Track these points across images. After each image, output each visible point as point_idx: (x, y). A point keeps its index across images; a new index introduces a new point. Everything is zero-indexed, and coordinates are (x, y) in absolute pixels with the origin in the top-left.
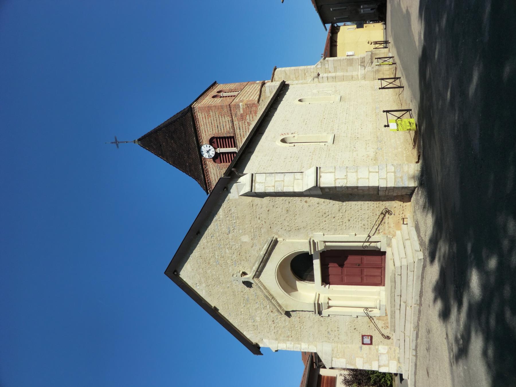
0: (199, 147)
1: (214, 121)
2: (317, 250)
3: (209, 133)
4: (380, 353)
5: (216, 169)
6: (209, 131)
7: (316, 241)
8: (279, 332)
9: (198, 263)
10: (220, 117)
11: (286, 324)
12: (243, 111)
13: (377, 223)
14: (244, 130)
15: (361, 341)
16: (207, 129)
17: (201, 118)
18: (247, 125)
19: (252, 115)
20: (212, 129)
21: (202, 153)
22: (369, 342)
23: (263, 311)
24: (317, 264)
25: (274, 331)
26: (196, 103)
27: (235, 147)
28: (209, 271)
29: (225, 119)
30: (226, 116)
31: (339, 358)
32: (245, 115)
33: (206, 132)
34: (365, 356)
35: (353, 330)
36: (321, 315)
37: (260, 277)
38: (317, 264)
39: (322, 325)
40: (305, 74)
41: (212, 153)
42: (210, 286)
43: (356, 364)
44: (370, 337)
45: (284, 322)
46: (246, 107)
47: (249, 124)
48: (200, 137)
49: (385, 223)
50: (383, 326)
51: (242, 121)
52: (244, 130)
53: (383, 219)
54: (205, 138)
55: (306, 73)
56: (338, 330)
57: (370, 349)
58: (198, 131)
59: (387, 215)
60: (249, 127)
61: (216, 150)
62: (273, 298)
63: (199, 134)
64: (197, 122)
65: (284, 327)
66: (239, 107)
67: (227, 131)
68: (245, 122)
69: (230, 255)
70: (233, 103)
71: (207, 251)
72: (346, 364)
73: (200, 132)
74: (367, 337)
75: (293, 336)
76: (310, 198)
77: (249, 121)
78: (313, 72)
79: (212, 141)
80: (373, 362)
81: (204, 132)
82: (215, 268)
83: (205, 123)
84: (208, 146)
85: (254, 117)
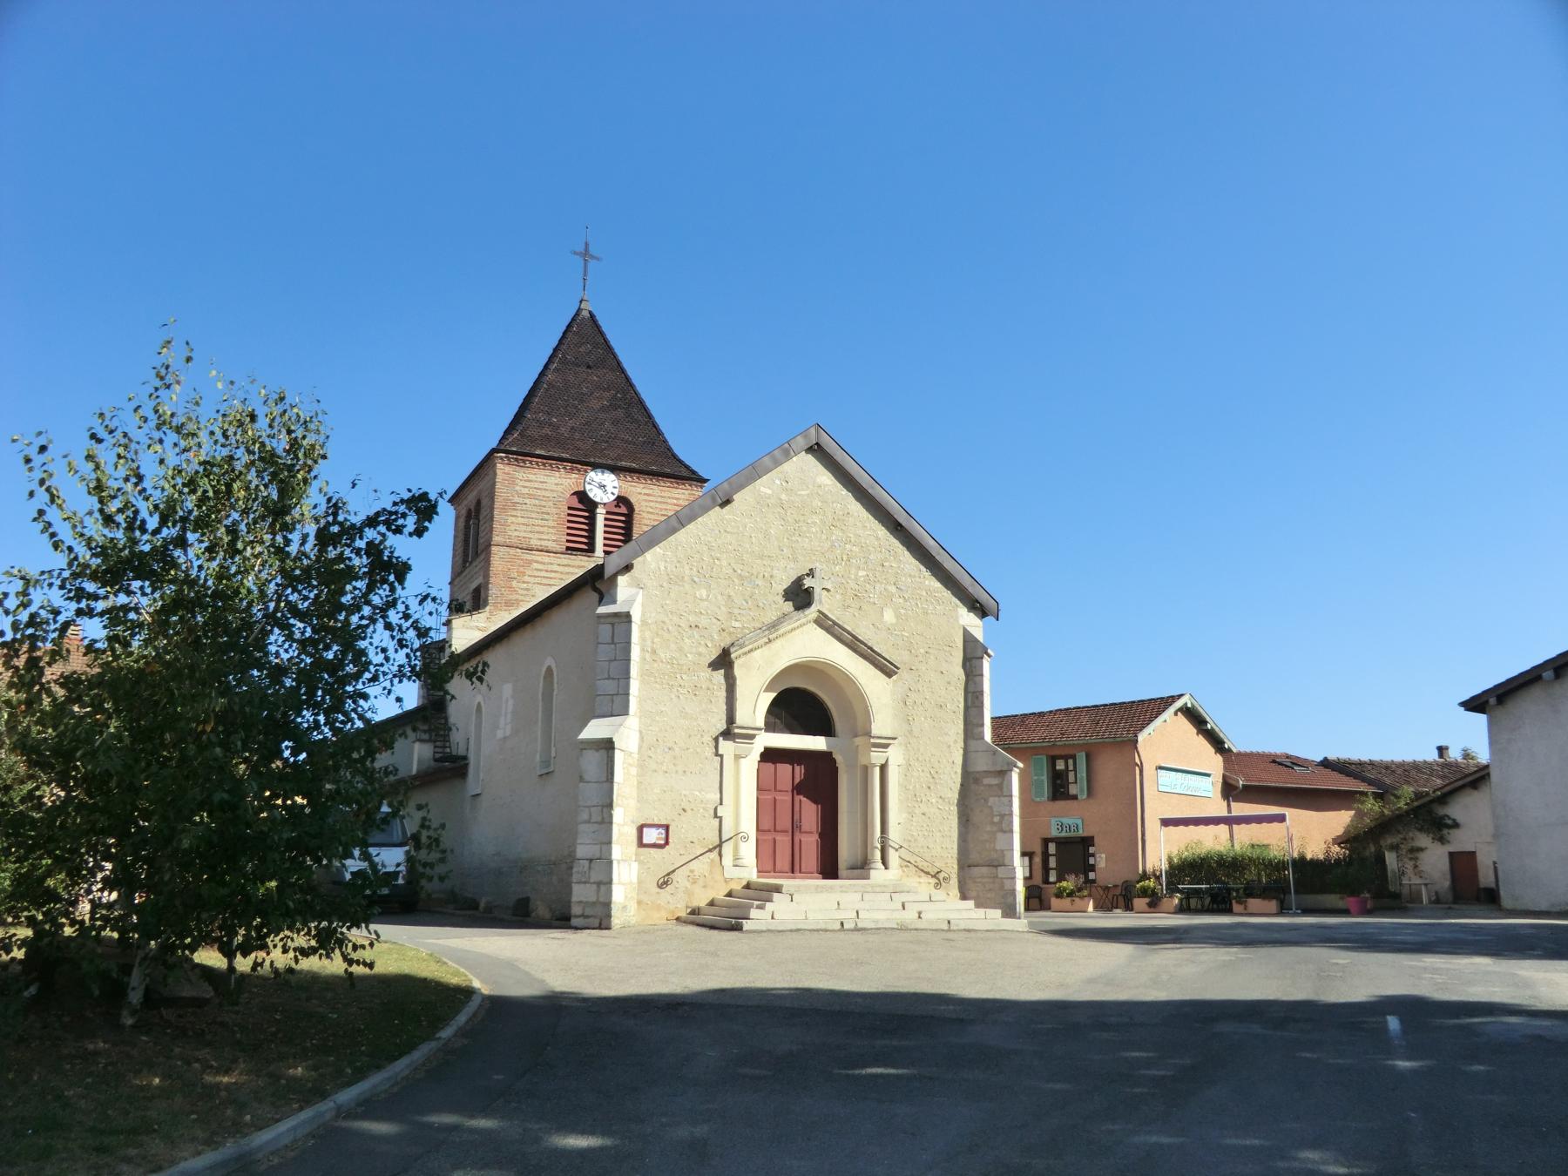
0: (614, 469)
2: (873, 749)
5: (558, 491)
6: (647, 504)
7: (889, 749)
8: (666, 635)
9: (835, 505)
11: (688, 655)
13: (922, 864)
15: (649, 822)
16: (652, 501)
17: (677, 496)
20: (651, 513)
21: (600, 470)
22: (645, 841)
23: (723, 608)
24: (817, 743)
25: (666, 620)
28: (816, 519)
33: (646, 497)
35: (680, 805)
36: (721, 739)
37: (815, 626)
38: (817, 743)
39: (690, 736)
41: (595, 494)
42: (782, 511)
44: (662, 842)
45: (694, 650)
48: (638, 478)
49: (920, 877)
50: (696, 873)
53: (928, 873)
54: (633, 489)
56: (677, 772)
58: (651, 480)
59: (933, 881)
62: (770, 641)
63: (645, 479)
64: (671, 483)
65: (681, 649)
69: (853, 577)
71: (860, 532)
73: (649, 482)
74: (664, 836)
75: (656, 665)
76: (961, 751)
82: (824, 537)
83: (665, 500)
84: (616, 492)
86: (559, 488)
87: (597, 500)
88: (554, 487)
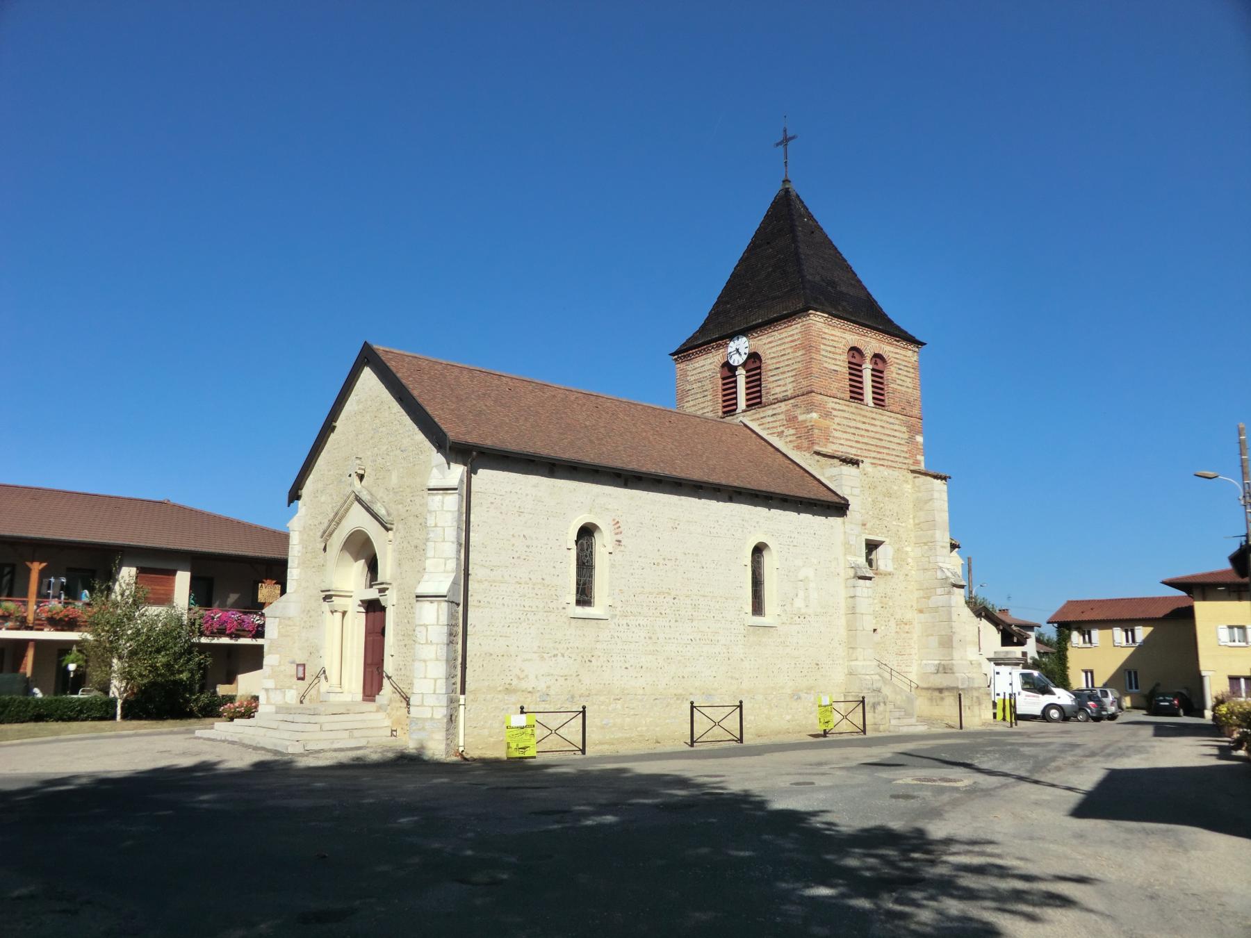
0: (745, 332)
1: (788, 360)
3: (768, 352)
4: (285, 691)
6: (770, 351)
12: (802, 421)
14: (771, 425)
16: (774, 347)
17: (791, 333)
18: (780, 429)
21: (736, 338)
26: (828, 318)
27: (748, 406)
29: (790, 383)
30: (794, 384)
31: (279, 629)
32: (794, 426)
33: (771, 345)
34: (282, 668)
41: (737, 360)
43: (270, 656)
46: (808, 426)
47: (780, 434)
48: (761, 331)
51: (786, 420)
52: (771, 425)
54: (760, 343)
57: (291, 676)
58: (770, 328)
60: (776, 435)
61: (740, 367)
63: (765, 330)
64: (785, 323)
66: (808, 413)
67: (770, 389)
68: (784, 425)
70: (820, 397)
72: (271, 639)
73: (770, 331)
77: (785, 434)
78: (929, 562)
79: (754, 357)
80: (273, 680)
81: (770, 340)
83: (783, 341)
84: (747, 351)
85: (791, 445)
86: (712, 367)
87: (736, 364)
88: (709, 367)
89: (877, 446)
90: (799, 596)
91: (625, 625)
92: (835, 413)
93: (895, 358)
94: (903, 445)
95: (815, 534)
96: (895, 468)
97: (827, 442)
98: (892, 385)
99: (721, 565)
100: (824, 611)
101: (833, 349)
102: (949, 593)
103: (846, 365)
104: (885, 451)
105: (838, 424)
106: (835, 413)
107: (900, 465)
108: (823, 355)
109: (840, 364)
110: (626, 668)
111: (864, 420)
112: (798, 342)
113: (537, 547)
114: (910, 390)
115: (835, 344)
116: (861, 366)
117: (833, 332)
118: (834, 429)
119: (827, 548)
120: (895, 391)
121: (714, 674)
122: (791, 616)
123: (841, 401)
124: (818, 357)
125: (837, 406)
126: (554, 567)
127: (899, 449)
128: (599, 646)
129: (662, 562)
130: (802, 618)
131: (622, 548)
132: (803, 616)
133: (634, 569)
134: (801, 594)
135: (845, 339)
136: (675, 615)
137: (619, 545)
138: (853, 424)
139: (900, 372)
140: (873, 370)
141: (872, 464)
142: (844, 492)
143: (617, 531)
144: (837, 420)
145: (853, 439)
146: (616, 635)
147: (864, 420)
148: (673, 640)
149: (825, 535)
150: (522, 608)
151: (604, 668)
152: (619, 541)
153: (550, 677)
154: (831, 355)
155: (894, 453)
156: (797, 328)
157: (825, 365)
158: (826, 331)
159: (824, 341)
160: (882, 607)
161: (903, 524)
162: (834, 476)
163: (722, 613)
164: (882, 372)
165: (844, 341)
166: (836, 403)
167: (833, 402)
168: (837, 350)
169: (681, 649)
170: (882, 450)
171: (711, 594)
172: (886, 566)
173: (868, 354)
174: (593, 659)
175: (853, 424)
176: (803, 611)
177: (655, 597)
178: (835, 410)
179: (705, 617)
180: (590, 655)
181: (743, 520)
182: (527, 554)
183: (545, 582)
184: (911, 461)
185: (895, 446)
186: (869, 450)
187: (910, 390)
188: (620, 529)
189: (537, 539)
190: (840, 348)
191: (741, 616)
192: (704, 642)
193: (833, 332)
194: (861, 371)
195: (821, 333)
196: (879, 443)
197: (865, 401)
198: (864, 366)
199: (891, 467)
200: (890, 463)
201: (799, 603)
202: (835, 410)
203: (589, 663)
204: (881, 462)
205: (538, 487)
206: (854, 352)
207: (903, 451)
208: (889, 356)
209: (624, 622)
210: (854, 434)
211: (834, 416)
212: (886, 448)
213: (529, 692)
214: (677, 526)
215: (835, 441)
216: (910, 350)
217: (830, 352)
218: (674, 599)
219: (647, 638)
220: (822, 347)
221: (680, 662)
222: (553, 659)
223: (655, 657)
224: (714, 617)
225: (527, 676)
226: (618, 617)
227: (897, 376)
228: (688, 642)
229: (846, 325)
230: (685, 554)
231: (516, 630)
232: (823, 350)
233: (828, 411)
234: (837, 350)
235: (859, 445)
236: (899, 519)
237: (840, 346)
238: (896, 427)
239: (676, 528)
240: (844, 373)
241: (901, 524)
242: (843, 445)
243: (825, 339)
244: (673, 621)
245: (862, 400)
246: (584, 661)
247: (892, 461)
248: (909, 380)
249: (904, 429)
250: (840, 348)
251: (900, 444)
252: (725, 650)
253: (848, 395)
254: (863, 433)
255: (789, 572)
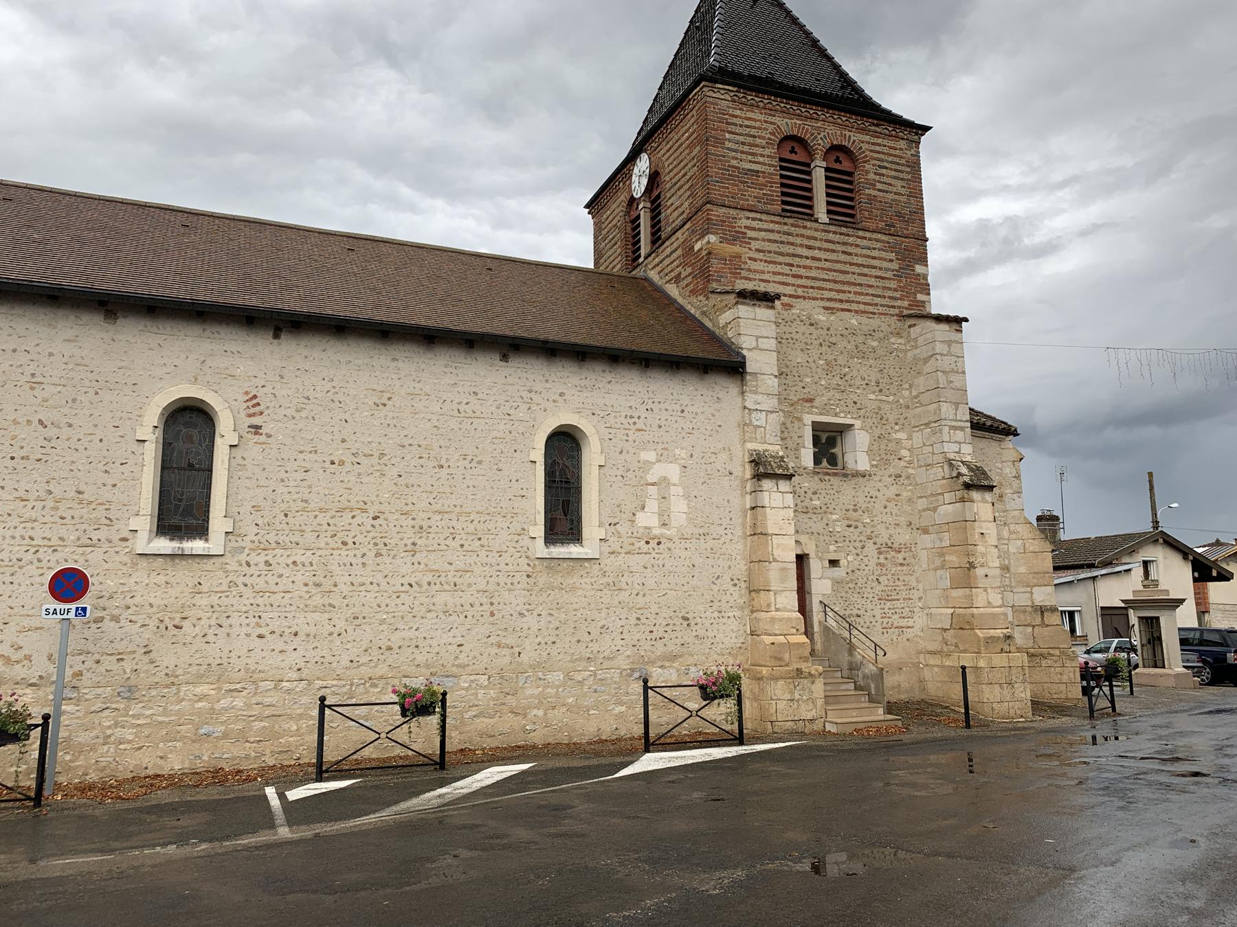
10: (689, 184)
19: (690, 283)
26: (739, 92)
40: (927, 425)
55: (929, 430)
70: (724, 210)
78: (933, 454)
89: (836, 282)
90: (646, 510)
91: (262, 566)
92: (750, 234)
93: (871, 151)
94: (889, 279)
95: (683, 411)
96: (874, 313)
97: (736, 278)
98: (867, 191)
99: (480, 462)
100: (701, 531)
101: (750, 140)
102: (962, 500)
103: (775, 162)
104: (852, 289)
105: (758, 251)
106: (750, 234)
107: (881, 310)
108: (728, 149)
109: (765, 161)
110: (261, 636)
111: (811, 243)
112: (695, 135)
113: (68, 440)
114: (903, 199)
115: (753, 132)
116: (808, 165)
117: (749, 115)
118: (750, 259)
119: (708, 433)
120: (872, 199)
121: (459, 640)
122: (630, 540)
123: (764, 217)
124: (720, 151)
125: (755, 224)
126: (106, 472)
127: (880, 284)
128: (203, 601)
129: (349, 459)
130: (653, 544)
131: (263, 438)
132: (656, 541)
133: (287, 472)
134: (652, 505)
135: (774, 124)
136: (376, 544)
137: (256, 433)
138: (790, 249)
139: (884, 171)
140: (827, 170)
141: (825, 308)
142: (746, 343)
143: (252, 410)
144: (755, 245)
145: (788, 272)
146: (240, 580)
147: (811, 243)
148: (370, 587)
149: (703, 413)
150: (27, 541)
151: (210, 638)
152: (258, 427)
153: (82, 658)
154: (746, 148)
155: (871, 291)
156: (693, 116)
157: (734, 163)
158: (738, 112)
159: (732, 128)
160: (849, 526)
161: (891, 398)
162: (730, 323)
163: (480, 539)
164: (850, 174)
165: (771, 128)
166: (753, 219)
167: (748, 218)
168: (758, 141)
169: (388, 601)
170: (846, 288)
171: (458, 509)
172: (856, 462)
173: (820, 143)
174: (186, 624)
175: (790, 249)
176: (656, 532)
177: (333, 517)
178: (754, 229)
179: (441, 547)
180: (178, 616)
181: (530, 391)
182: (44, 451)
183: (85, 496)
184: (906, 304)
185: (872, 281)
186: (819, 288)
187: (903, 199)
188: (257, 409)
189: (70, 425)
190: (764, 138)
191: (522, 543)
192: (438, 587)
193: (749, 115)
194: (809, 173)
195: (727, 116)
196: (841, 277)
197: (815, 216)
198: (813, 165)
199: (865, 312)
200: (862, 307)
201: (648, 519)
202: (754, 229)
203: (175, 631)
204: (845, 306)
205: (74, 341)
206: (794, 144)
207: (890, 289)
208: (861, 148)
209: (262, 559)
210: (792, 265)
211: (750, 238)
212: (855, 284)
213: (31, 685)
214: (386, 402)
215: (751, 276)
216: (903, 139)
217: (743, 143)
218: (375, 518)
219: (311, 583)
220: (727, 136)
221: (383, 622)
222: (94, 626)
223: (327, 616)
224: (462, 546)
225: (28, 658)
226: (247, 551)
227: (877, 178)
228: (403, 589)
229: (775, 103)
230: (404, 446)
231: (10, 579)
232: (729, 140)
233: (738, 232)
234: (758, 141)
235: (799, 282)
236: (881, 391)
237: (763, 134)
238: (875, 253)
239: (385, 405)
240: (772, 174)
241: (885, 398)
242: (769, 282)
243: (736, 125)
244: (371, 554)
245: (812, 215)
246: (162, 626)
247: (865, 304)
248: (900, 183)
249: (892, 256)
250: (764, 138)
251: (883, 278)
252: (484, 600)
253: (778, 208)
254: (808, 262)
255: (628, 470)
